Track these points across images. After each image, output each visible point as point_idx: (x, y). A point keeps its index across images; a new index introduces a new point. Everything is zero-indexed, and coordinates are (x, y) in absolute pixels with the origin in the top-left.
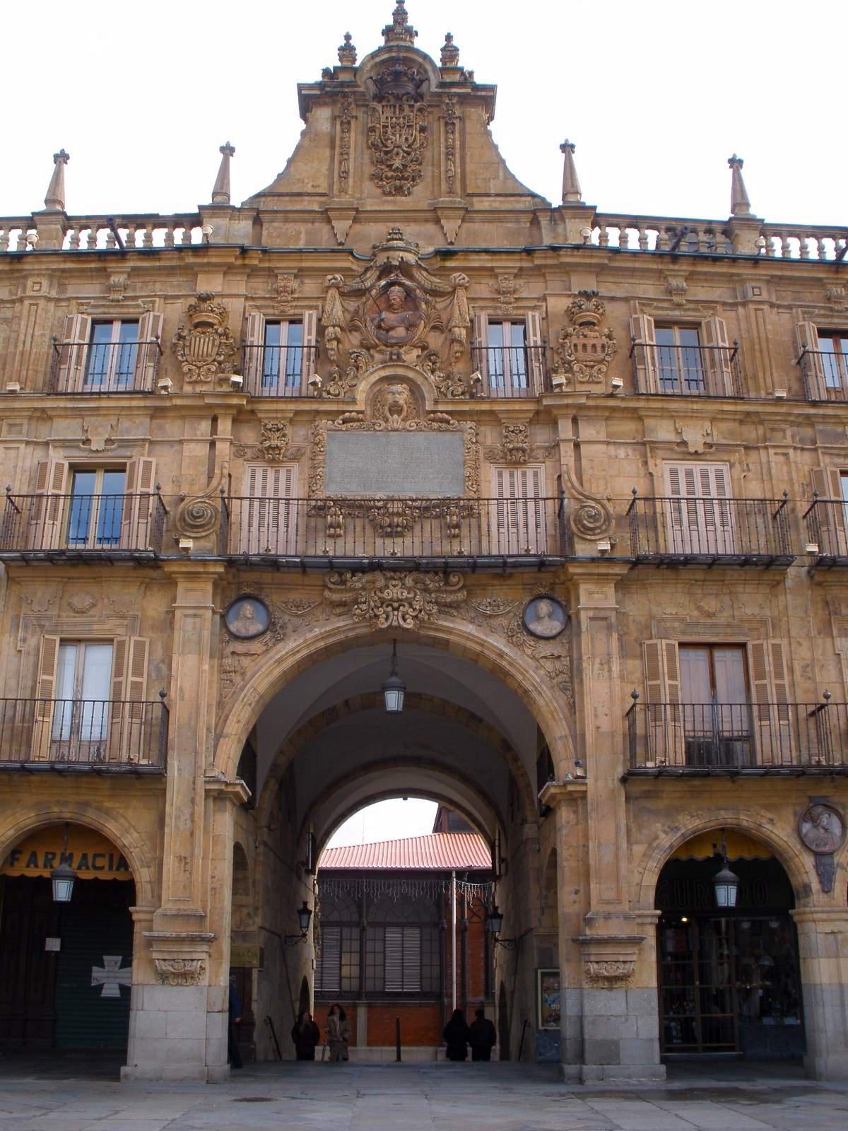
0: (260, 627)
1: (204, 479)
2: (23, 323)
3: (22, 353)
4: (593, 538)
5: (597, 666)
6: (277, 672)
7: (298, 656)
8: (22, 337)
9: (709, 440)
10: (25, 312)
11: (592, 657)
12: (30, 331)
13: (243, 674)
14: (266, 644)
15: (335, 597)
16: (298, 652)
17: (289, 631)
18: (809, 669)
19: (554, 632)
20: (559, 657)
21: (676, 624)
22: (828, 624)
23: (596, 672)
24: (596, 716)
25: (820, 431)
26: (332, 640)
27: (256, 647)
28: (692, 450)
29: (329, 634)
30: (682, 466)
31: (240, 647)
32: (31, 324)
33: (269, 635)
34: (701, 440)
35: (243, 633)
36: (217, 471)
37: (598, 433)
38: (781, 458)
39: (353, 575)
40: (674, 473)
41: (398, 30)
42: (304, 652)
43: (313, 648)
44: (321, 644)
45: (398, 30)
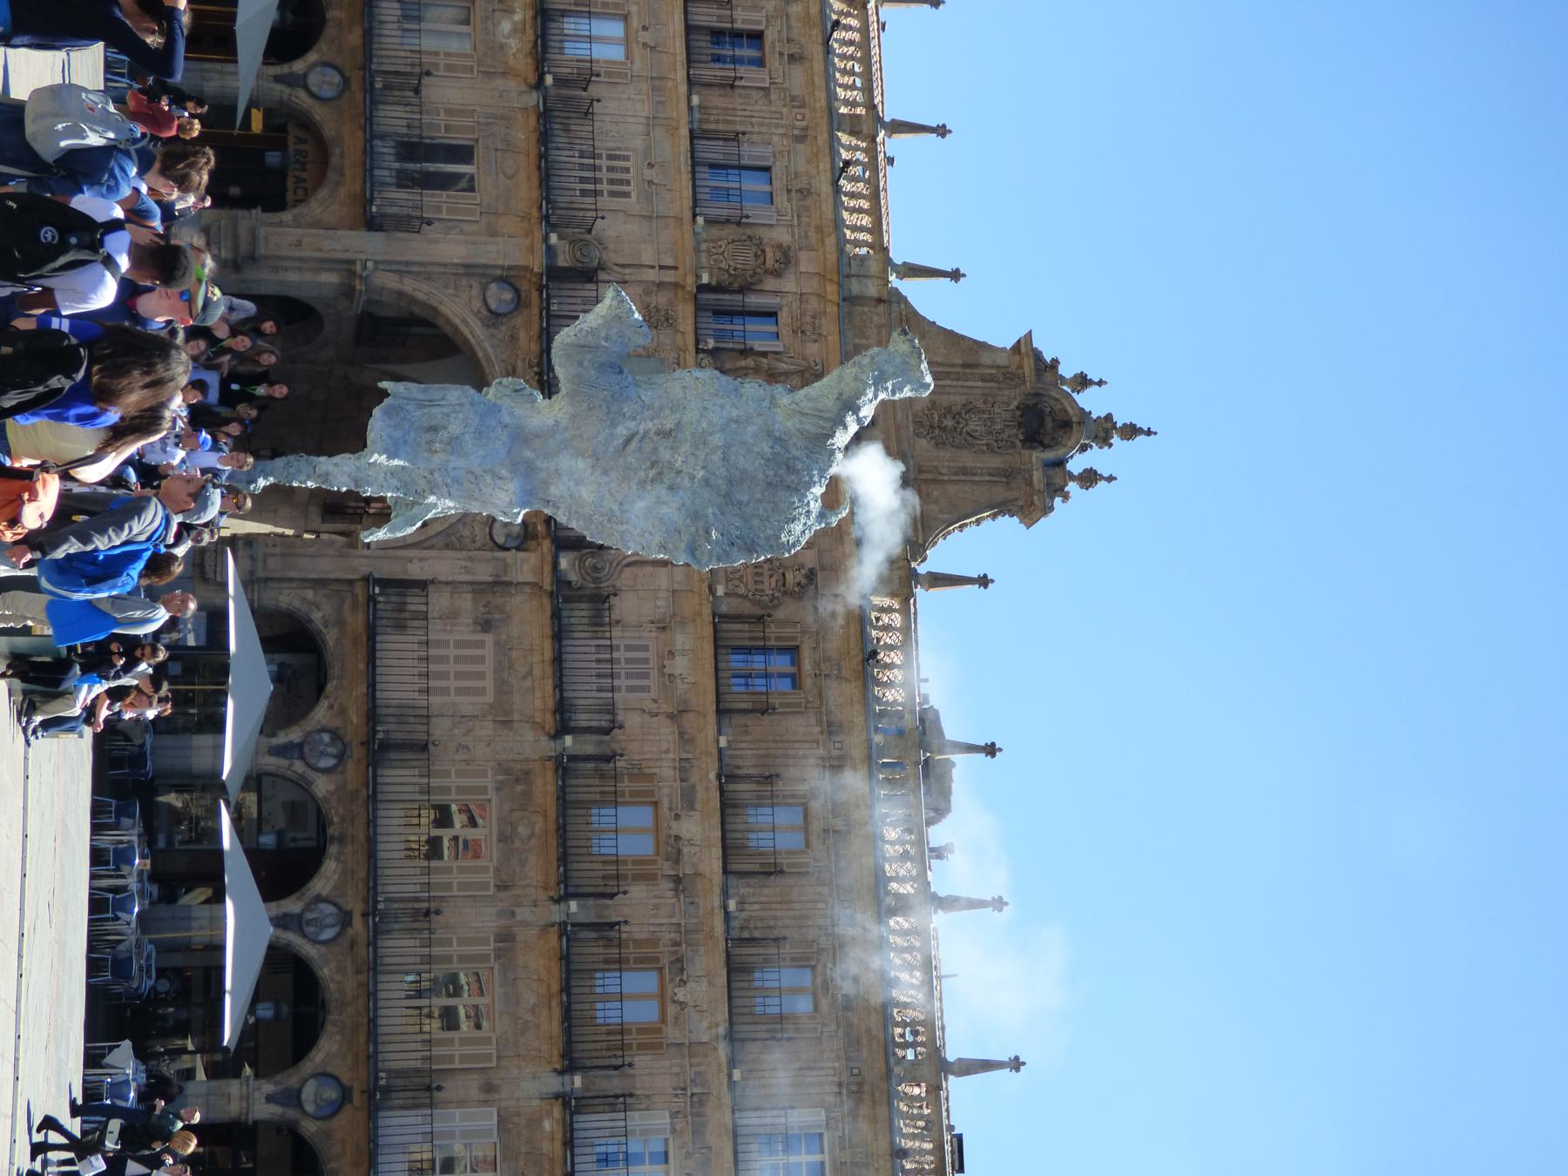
0: (493, 306)
1: (621, 261)
2: (764, 108)
3: (734, 109)
4: (577, 566)
5: (464, 564)
6: (457, 321)
7: (470, 337)
8: (750, 108)
9: (678, 681)
10: (773, 109)
11: (470, 559)
12: (756, 114)
13: (455, 296)
14: (479, 312)
15: (519, 363)
16: (473, 336)
17: (492, 330)
18: (465, 750)
19: (496, 537)
20: (474, 542)
21: (504, 637)
22: (508, 772)
23: (458, 562)
24: (421, 560)
25: (693, 787)
26: (484, 363)
27: (477, 305)
28: (666, 663)
29: (488, 359)
30: (650, 655)
31: (475, 291)
32: (762, 114)
33: (485, 313)
34: (677, 671)
35: (489, 294)
36: (627, 271)
37: (679, 583)
38: (664, 748)
39: (536, 373)
40: (646, 648)
41: (1104, 432)
42: (473, 341)
43: (477, 348)
44: (480, 355)
45: (1104, 432)
